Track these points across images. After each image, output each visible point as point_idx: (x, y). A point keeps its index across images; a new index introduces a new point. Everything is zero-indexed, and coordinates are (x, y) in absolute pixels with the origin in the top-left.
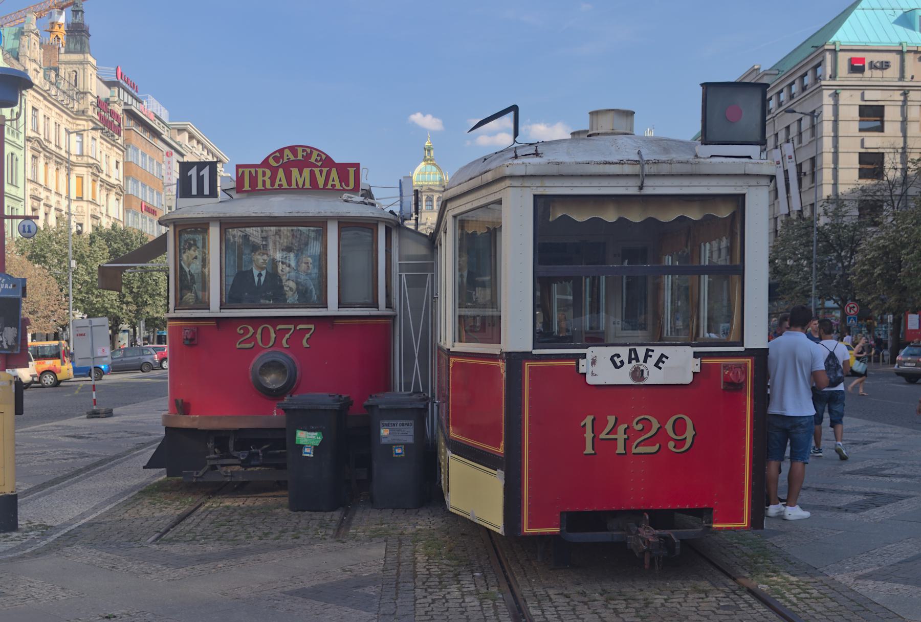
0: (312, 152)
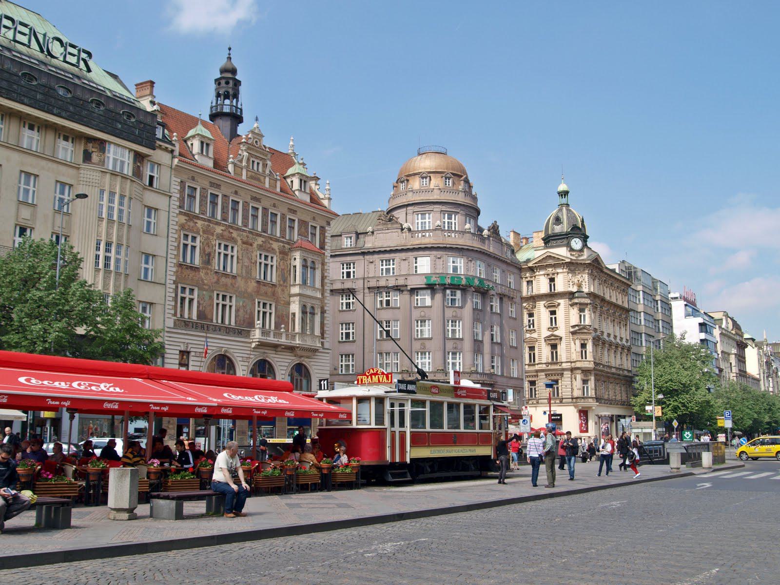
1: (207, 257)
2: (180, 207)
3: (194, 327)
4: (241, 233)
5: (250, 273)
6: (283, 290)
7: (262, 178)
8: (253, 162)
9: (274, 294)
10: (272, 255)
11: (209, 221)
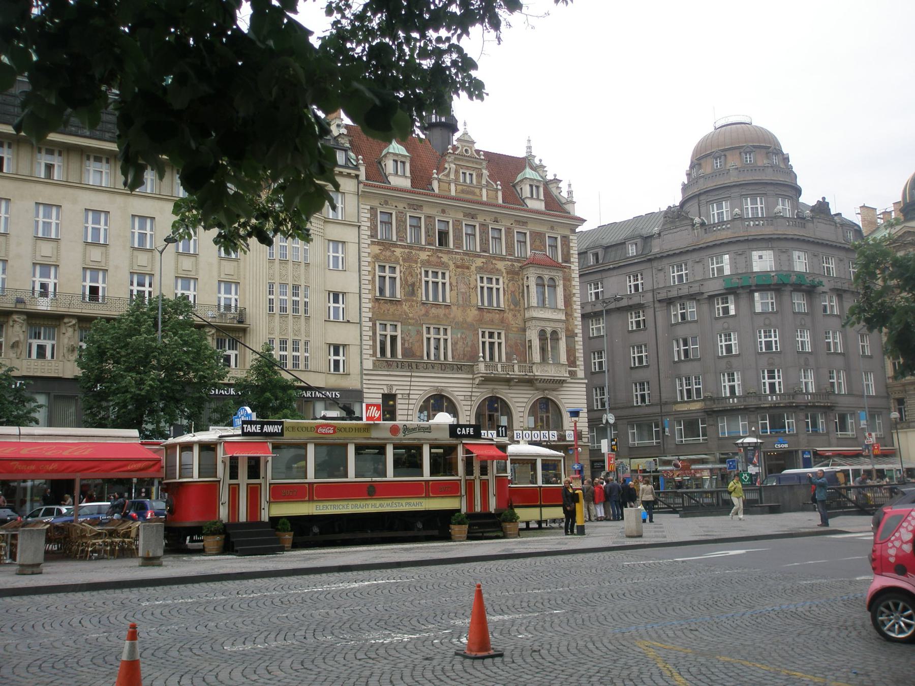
1: (411, 288)
2: (372, 236)
3: (400, 366)
4: (454, 256)
6: (515, 316)
7: (477, 191)
8: (464, 174)
9: (502, 321)
11: (411, 247)
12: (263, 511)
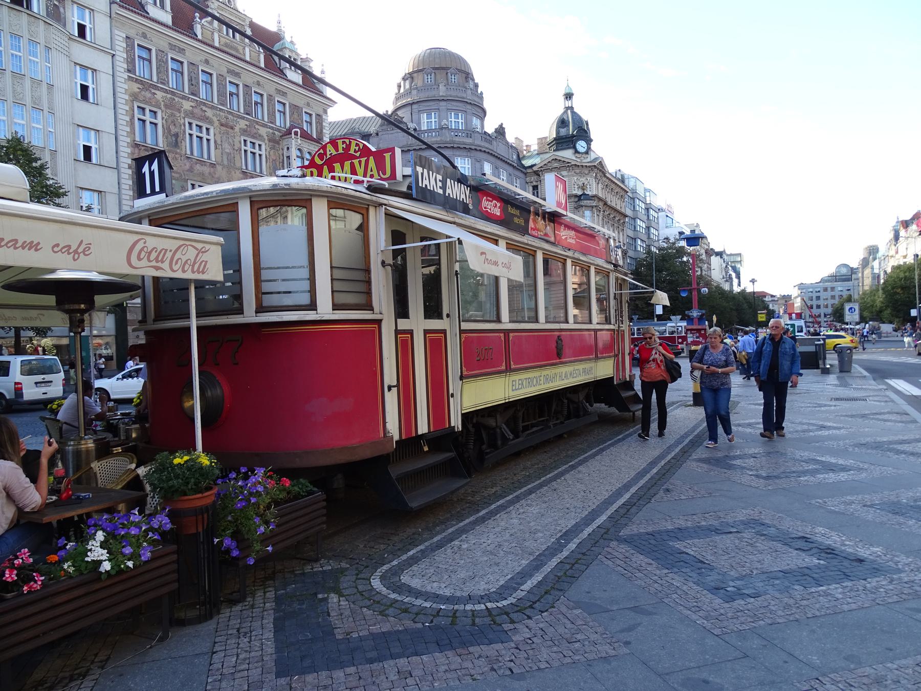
0: (350, 142)
1: (174, 139)
4: (218, 112)
5: (233, 161)
7: (240, 48)
10: (260, 143)
12: (451, 400)
